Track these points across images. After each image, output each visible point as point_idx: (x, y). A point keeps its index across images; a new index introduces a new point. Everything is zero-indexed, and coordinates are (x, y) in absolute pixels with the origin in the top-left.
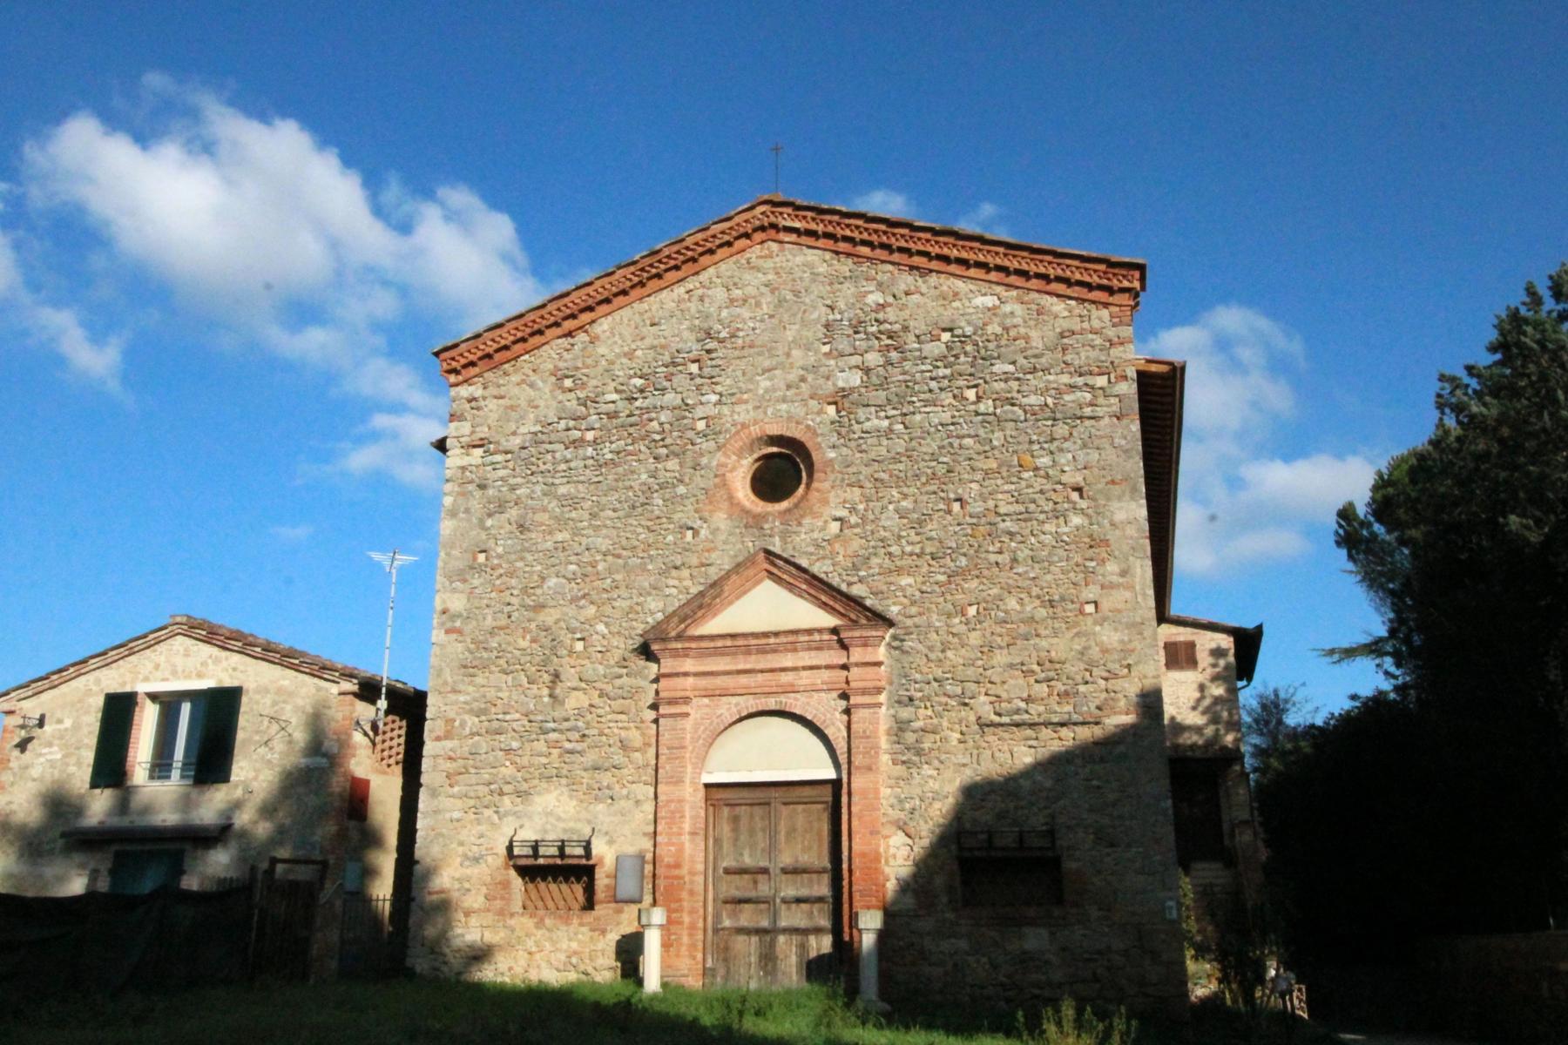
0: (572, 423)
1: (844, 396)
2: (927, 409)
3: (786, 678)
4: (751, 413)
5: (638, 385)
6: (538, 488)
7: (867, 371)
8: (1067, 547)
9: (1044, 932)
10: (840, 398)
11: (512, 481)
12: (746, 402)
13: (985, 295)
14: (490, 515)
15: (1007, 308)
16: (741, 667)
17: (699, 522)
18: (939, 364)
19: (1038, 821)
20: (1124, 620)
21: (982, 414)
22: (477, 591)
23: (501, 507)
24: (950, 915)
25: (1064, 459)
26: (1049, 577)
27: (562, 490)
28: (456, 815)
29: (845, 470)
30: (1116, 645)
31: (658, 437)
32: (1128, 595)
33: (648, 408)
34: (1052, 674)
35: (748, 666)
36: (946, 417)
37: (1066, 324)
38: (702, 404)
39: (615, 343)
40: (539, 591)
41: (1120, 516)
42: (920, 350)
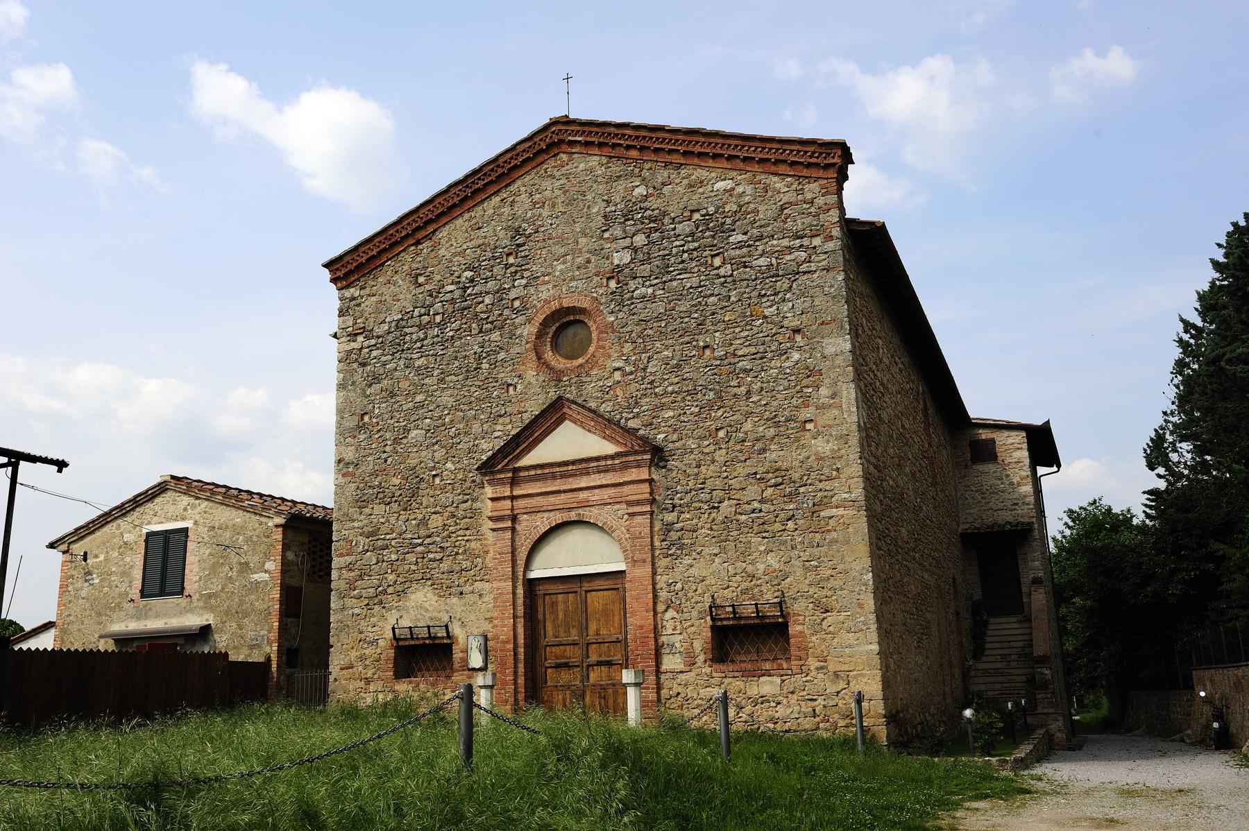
0: (423, 311)
1: (619, 272)
2: (682, 277)
3: (583, 495)
4: (551, 292)
5: (469, 277)
6: (402, 363)
7: (635, 250)
9: (778, 680)
10: (616, 272)
11: (384, 359)
12: (548, 282)
13: (725, 180)
14: (370, 386)
15: (740, 189)
16: (549, 489)
17: (516, 380)
18: (690, 239)
19: (770, 596)
21: (724, 277)
22: (362, 444)
23: (376, 379)
24: (708, 670)
25: (786, 307)
26: (775, 403)
27: (418, 363)
28: (357, 611)
29: (621, 330)
30: (828, 453)
31: (484, 316)
32: (836, 412)
33: (476, 294)
34: (780, 480)
35: (554, 489)
36: (695, 281)
37: (785, 199)
38: (514, 287)
39: (452, 245)
40: (404, 441)
41: (829, 350)
42: (674, 229)
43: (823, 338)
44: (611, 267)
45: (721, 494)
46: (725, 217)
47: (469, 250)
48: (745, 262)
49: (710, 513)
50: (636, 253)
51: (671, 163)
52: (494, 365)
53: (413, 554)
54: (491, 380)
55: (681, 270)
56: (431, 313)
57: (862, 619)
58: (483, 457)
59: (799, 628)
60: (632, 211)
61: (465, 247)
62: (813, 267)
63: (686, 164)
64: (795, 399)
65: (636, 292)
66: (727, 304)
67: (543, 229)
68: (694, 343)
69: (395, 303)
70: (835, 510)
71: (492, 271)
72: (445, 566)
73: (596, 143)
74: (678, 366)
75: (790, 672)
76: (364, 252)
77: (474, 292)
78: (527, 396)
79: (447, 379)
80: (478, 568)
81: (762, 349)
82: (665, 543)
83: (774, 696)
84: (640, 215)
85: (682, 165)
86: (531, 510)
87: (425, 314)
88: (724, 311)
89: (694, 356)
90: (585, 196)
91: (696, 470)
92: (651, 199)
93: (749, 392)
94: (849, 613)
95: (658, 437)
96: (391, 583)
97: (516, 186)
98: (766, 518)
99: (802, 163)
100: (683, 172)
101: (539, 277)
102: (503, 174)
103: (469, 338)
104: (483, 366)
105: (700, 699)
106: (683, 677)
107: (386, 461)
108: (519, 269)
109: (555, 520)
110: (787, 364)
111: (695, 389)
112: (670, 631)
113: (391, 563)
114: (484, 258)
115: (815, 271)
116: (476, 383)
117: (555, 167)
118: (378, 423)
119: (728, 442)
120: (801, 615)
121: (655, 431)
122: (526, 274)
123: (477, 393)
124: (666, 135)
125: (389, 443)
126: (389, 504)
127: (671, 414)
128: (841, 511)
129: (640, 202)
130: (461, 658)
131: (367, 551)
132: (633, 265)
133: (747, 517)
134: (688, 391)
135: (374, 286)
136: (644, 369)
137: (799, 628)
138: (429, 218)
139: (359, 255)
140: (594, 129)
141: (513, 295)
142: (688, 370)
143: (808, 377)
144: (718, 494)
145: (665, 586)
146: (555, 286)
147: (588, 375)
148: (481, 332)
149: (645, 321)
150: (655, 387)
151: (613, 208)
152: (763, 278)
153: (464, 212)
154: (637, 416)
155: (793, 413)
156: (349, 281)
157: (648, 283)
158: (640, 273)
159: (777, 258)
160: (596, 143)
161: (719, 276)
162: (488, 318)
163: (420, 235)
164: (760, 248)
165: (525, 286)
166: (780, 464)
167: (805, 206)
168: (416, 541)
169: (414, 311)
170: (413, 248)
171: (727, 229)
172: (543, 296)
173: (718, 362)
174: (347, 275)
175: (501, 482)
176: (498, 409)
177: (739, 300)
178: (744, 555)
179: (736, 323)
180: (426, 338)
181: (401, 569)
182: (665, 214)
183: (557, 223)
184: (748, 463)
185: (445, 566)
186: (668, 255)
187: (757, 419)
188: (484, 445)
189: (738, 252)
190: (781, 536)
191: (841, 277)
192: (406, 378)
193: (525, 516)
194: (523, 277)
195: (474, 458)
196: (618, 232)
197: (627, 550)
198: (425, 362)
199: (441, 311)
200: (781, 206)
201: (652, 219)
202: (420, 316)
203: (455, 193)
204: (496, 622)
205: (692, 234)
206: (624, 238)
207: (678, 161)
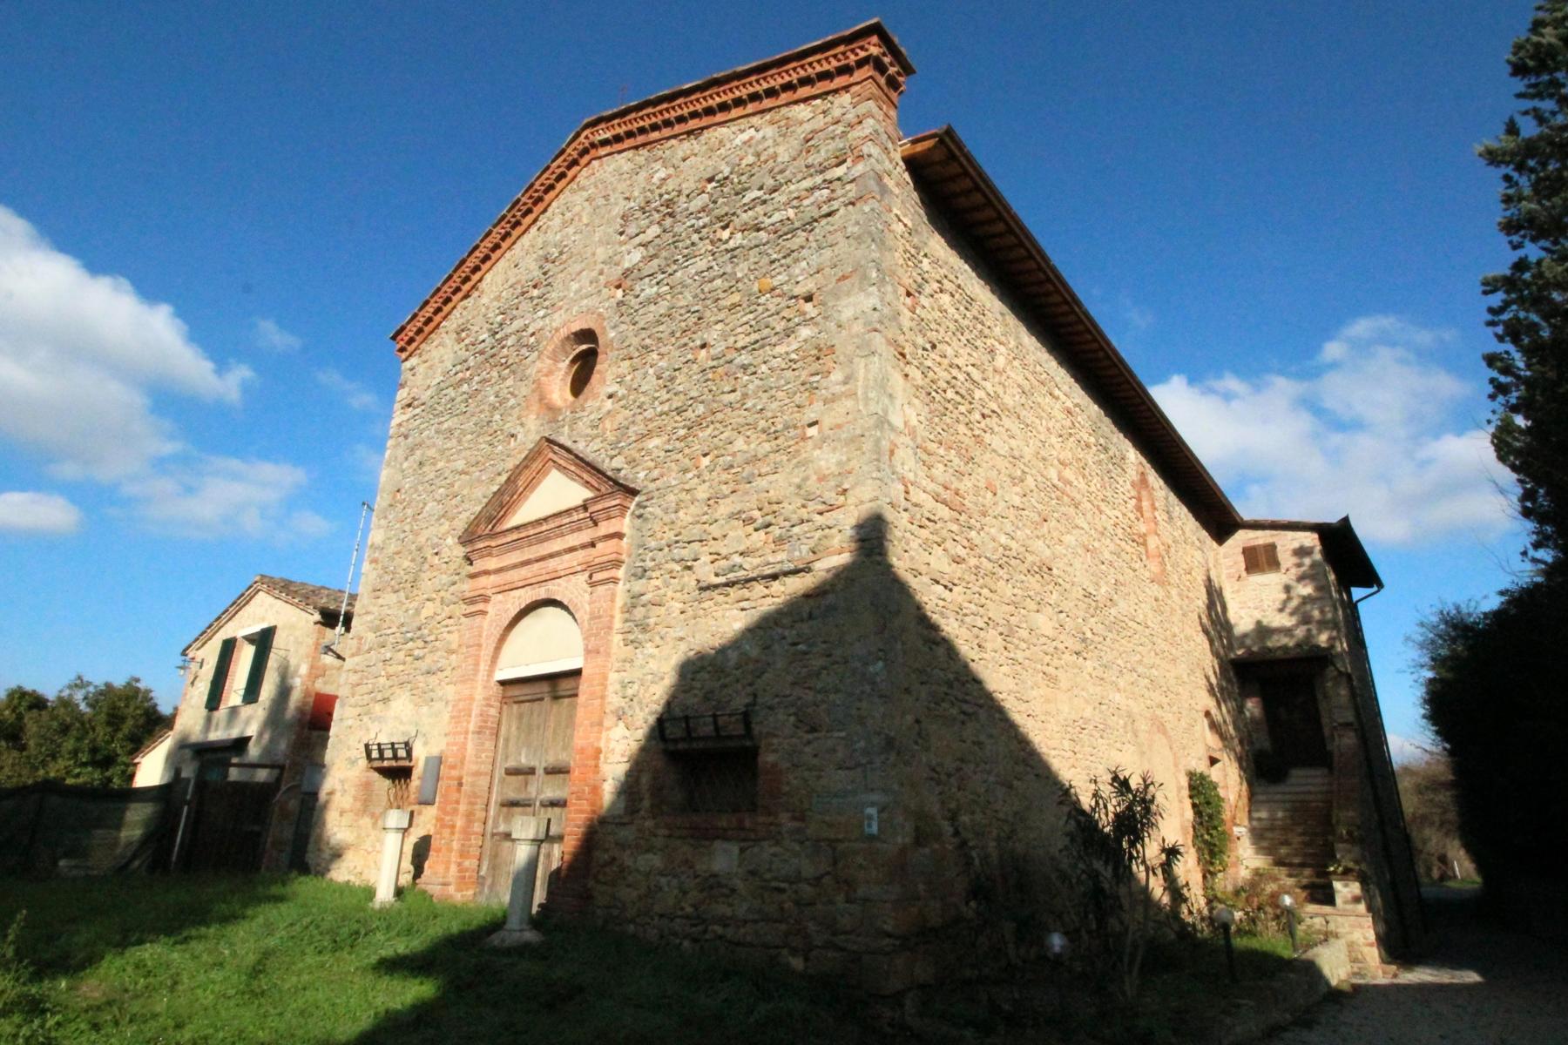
3: (552, 564)
8: (794, 366)
9: (735, 849)
19: (740, 702)
20: (844, 436)
32: (849, 403)
37: (808, 127)
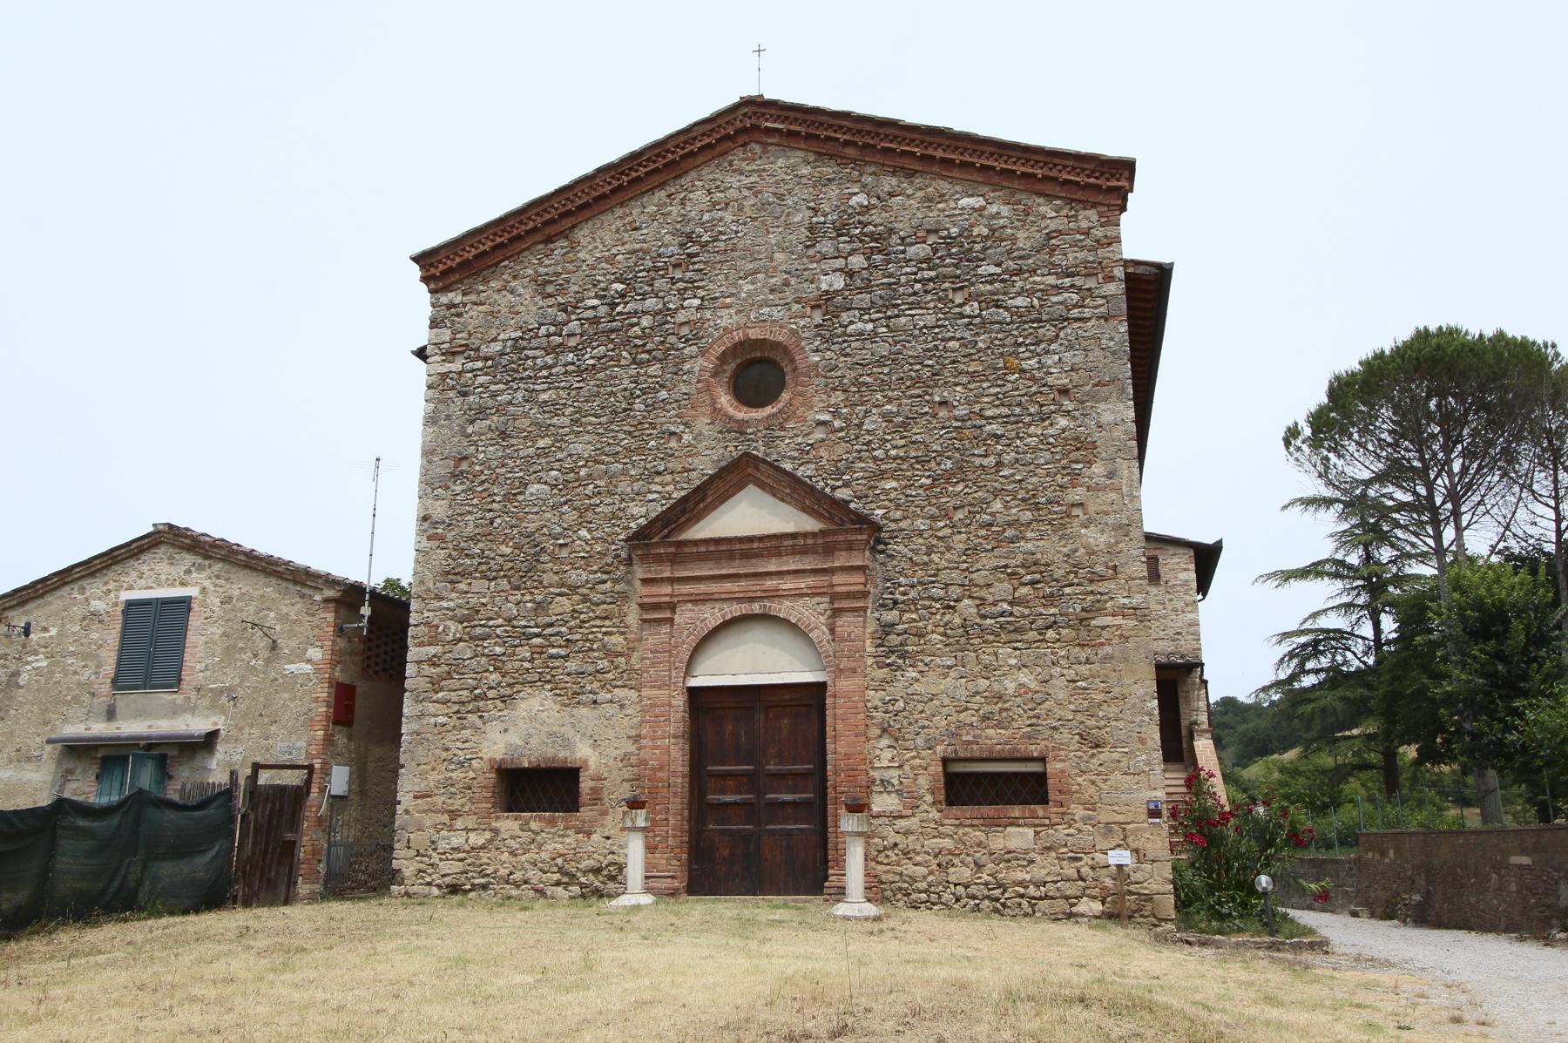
0: (552, 329)
1: (827, 300)
2: (913, 312)
3: (770, 583)
4: (734, 317)
5: (619, 289)
6: (519, 395)
7: (850, 274)
8: (1053, 450)
9: (1030, 832)
10: (825, 302)
11: (493, 388)
12: (728, 306)
13: (972, 196)
14: (472, 422)
15: (993, 209)
16: (724, 572)
17: (682, 428)
18: (924, 266)
20: (1110, 522)
21: (969, 317)
22: (458, 498)
23: (482, 412)
24: (934, 814)
25: (1050, 360)
26: (1034, 480)
27: (543, 397)
28: (441, 720)
29: (828, 374)
30: (1102, 546)
31: (640, 342)
32: (1114, 496)
33: (630, 313)
34: (1038, 576)
35: (732, 571)
36: (930, 320)
37: (1053, 225)
38: (684, 308)
39: (596, 247)
40: (520, 498)
41: (1107, 418)
42: (903, 252)
43: (1097, 402)
44: (817, 293)
45: (959, 590)
46: (972, 242)
47: (621, 256)
48: (998, 300)
49: (944, 614)
50: (851, 278)
51: (902, 168)
52: (651, 407)
53: (527, 648)
54: (647, 426)
55: (912, 303)
56: (564, 333)
57: (1144, 757)
58: (632, 525)
59: (1059, 765)
60: (847, 225)
61: (616, 252)
62: (1087, 312)
63: (921, 172)
64: (1059, 476)
65: (851, 327)
66: (972, 351)
67: (724, 238)
68: (927, 397)
69: (512, 316)
70: (1110, 618)
71: (652, 285)
72: (572, 666)
73: (803, 134)
74: (904, 425)
75: (1047, 821)
76: (472, 246)
77: (626, 310)
78: (695, 450)
79: (584, 420)
80: (619, 670)
81: (1018, 410)
82: (882, 649)
83: (1026, 851)
84: (858, 231)
85: (916, 171)
86: (698, 598)
87: (555, 334)
88: (967, 360)
89: (926, 413)
90: (783, 200)
91: (926, 558)
92: (874, 211)
93: (999, 464)
94: (1126, 750)
95: (877, 512)
96: (493, 684)
97: (689, 179)
98: (1018, 625)
99: (1077, 183)
100: (917, 181)
101: (716, 298)
102: (673, 162)
103: (616, 369)
104: (636, 407)
105: (925, 852)
106: (902, 823)
107: (492, 523)
108: (690, 285)
109: (731, 612)
110: (1051, 431)
111: (926, 456)
112: (885, 763)
113: (494, 658)
114: (642, 268)
115: (1090, 319)
116: (625, 428)
117: (744, 160)
118: (482, 472)
119: (969, 525)
120: (1063, 750)
121: (873, 505)
122: (701, 293)
123: (626, 441)
124: (897, 132)
125: (498, 499)
126: (495, 578)
127: (894, 484)
128: (1119, 620)
129: (859, 214)
130: (591, 789)
131: (460, 640)
132: (847, 293)
133: (993, 621)
134: (917, 457)
135: (483, 292)
136: (860, 425)
137: (1059, 765)
138: (567, 208)
139: (464, 250)
140: (798, 115)
141: (681, 317)
142: (918, 431)
143: (1078, 449)
144: (955, 591)
145: (880, 704)
146: (740, 311)
147: (782, 428)
148: (634, 361)
149: (861, 364)
150: (874, 450)
151: (822, 219)
152: (1020, 322)
153: (615, 206)
154: (846, 485)
155: (1058, 493)
156: (447, 282)
157: (866, 317)
158: (858, 304)
159: (1039, 299)
160: (803, 134)
161: (962, 316)
162: (644, 345)
163: (551, 230)
164: (1020, 284)
165: (698, 308)
166: (1039, 556)
167: (1078, 236)
168: (532, 630)
169: (539, 329)
170: (541, 246)
171: (975, 257)
172: (723, 323)
173: (959, 424)
174: (445, 273)
175: (659, 559)
176: (655, 463)
177: (989, 348)
178: (988, 671)
179: (984, 375)
180: (555, 365)
181: (509, 666)
182: (891, 231)
183: (745, 231)
184: (996, 552)
185: (572, 666)
186: (895, 283)
187: (1008, 498)
188: (636, 509)
189: (989, 287)
190: (1038, 648)
191: (1124, 328)
192: (526, 414)
193: (690, 605)
194: (695, 297)
195: (619, 526)
196: (826, 247)
197: (830, 656)
198: (554, 397)
199: (579, 331)
200: (1047, 234)
201: (874, 237)
202: (548, 336)
203: (605, 180)
204: (644, 742)
205: (927, 260)
206: (836, 258)
207: (912, 167)
